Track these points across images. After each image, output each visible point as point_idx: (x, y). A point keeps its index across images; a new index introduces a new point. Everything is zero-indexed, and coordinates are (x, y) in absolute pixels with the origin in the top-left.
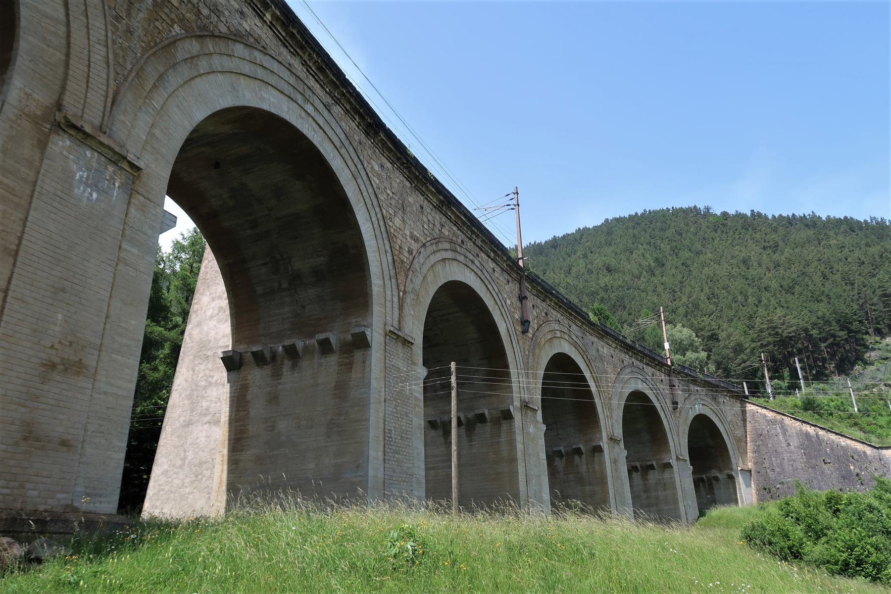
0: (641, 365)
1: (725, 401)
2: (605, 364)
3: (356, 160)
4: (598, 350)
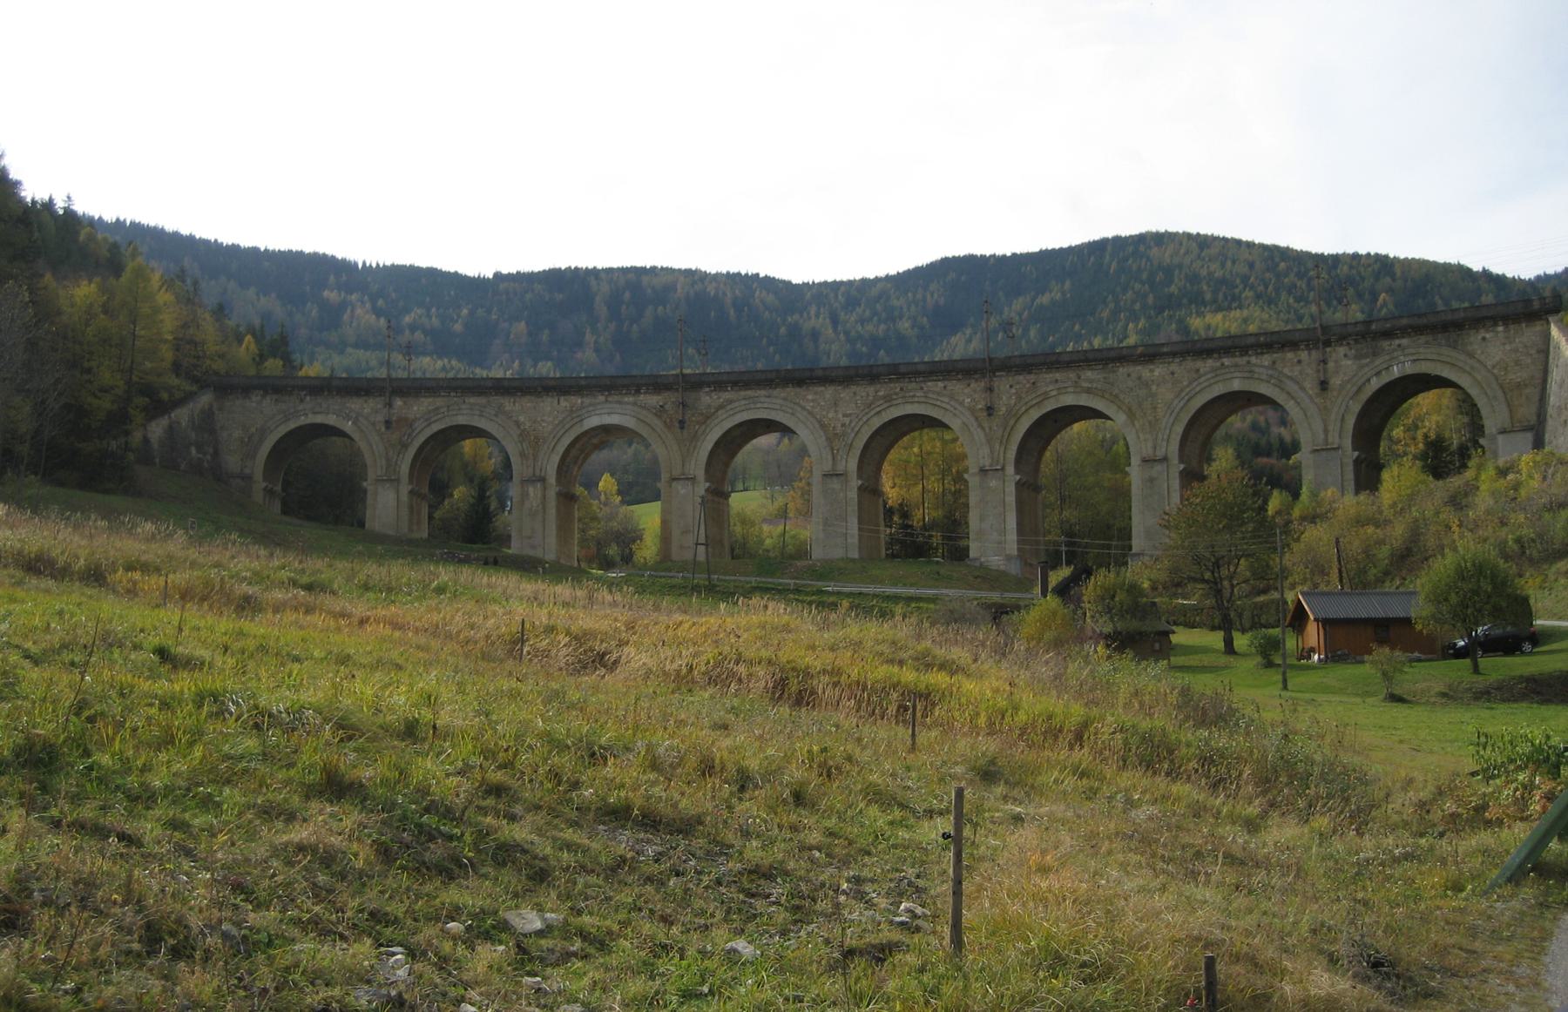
0: (1242, 361)
1: (1488, 336)
2: (1154, 387)
3: (792, 405)
4: (1139, 378)
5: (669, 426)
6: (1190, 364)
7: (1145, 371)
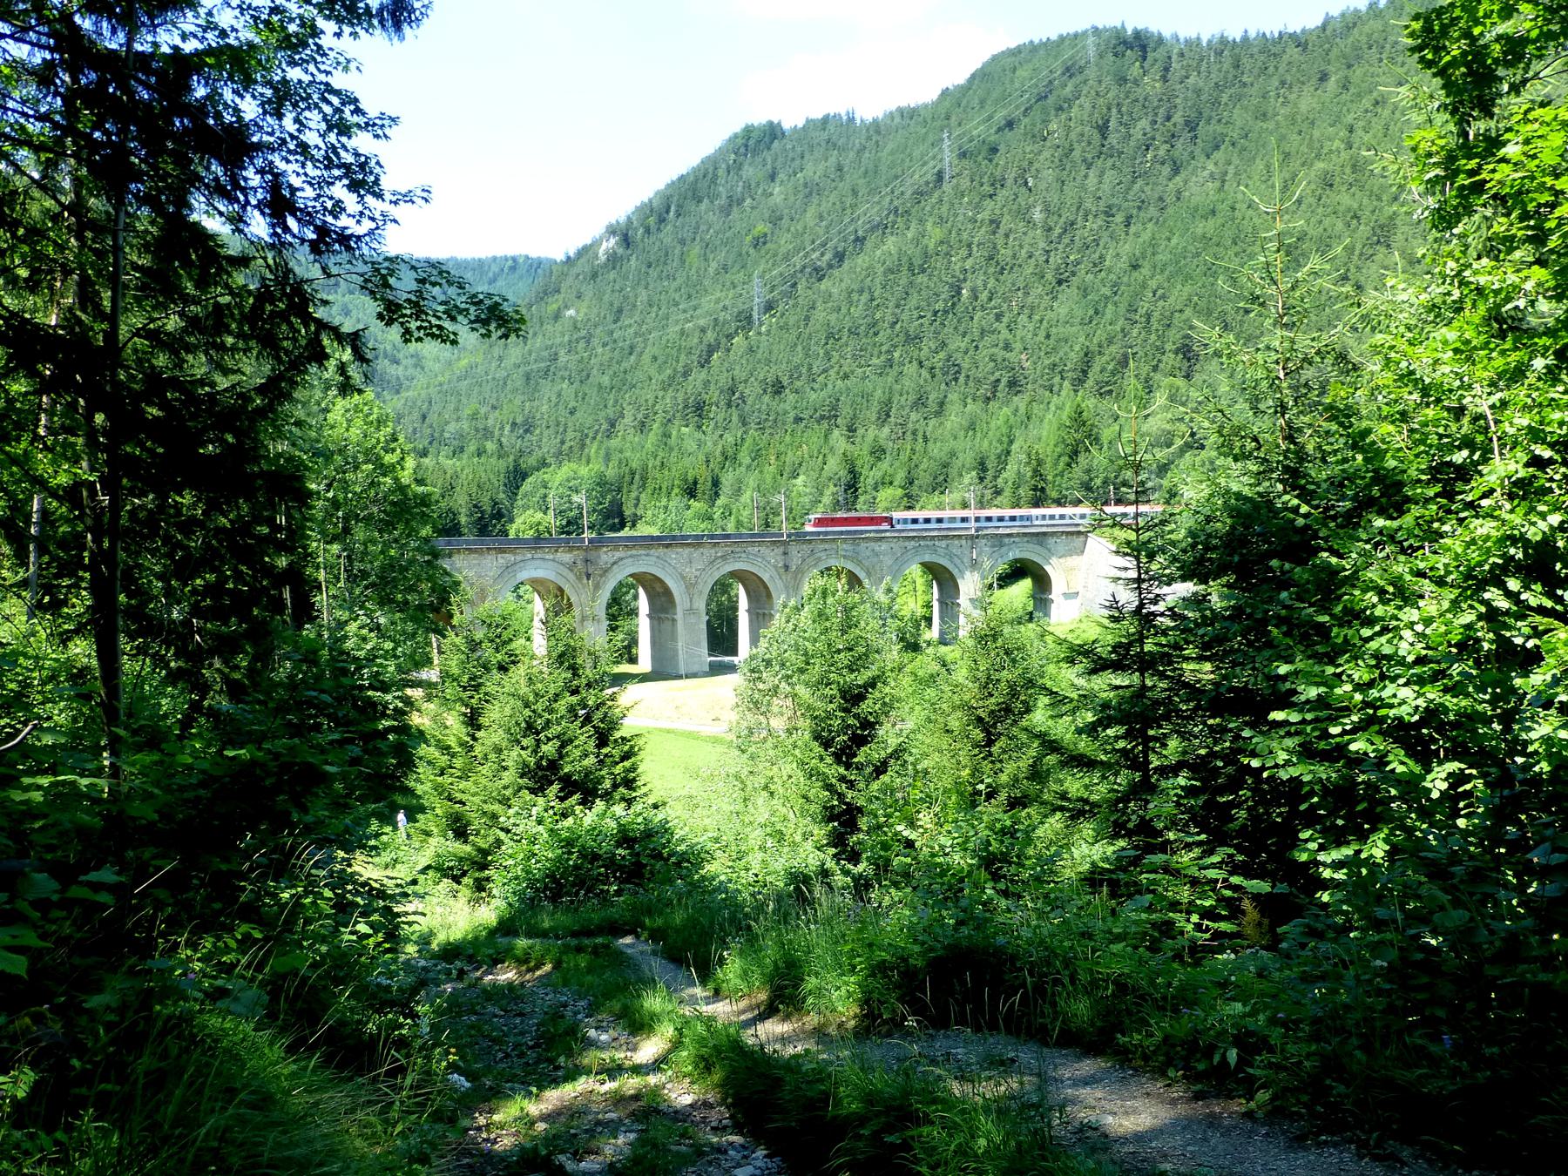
5: (579, 579)
6: (901, 543)
7: (876, 546)
